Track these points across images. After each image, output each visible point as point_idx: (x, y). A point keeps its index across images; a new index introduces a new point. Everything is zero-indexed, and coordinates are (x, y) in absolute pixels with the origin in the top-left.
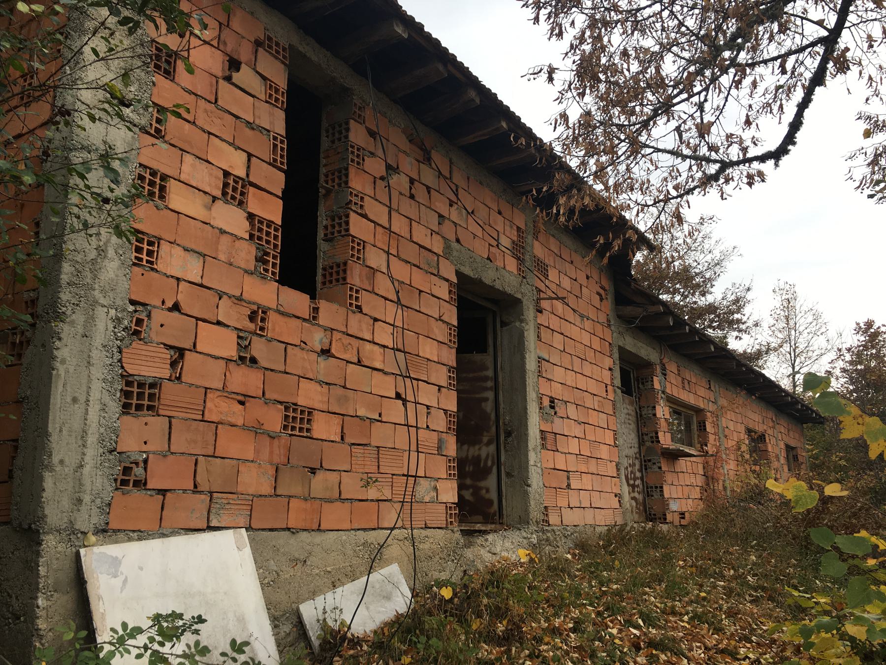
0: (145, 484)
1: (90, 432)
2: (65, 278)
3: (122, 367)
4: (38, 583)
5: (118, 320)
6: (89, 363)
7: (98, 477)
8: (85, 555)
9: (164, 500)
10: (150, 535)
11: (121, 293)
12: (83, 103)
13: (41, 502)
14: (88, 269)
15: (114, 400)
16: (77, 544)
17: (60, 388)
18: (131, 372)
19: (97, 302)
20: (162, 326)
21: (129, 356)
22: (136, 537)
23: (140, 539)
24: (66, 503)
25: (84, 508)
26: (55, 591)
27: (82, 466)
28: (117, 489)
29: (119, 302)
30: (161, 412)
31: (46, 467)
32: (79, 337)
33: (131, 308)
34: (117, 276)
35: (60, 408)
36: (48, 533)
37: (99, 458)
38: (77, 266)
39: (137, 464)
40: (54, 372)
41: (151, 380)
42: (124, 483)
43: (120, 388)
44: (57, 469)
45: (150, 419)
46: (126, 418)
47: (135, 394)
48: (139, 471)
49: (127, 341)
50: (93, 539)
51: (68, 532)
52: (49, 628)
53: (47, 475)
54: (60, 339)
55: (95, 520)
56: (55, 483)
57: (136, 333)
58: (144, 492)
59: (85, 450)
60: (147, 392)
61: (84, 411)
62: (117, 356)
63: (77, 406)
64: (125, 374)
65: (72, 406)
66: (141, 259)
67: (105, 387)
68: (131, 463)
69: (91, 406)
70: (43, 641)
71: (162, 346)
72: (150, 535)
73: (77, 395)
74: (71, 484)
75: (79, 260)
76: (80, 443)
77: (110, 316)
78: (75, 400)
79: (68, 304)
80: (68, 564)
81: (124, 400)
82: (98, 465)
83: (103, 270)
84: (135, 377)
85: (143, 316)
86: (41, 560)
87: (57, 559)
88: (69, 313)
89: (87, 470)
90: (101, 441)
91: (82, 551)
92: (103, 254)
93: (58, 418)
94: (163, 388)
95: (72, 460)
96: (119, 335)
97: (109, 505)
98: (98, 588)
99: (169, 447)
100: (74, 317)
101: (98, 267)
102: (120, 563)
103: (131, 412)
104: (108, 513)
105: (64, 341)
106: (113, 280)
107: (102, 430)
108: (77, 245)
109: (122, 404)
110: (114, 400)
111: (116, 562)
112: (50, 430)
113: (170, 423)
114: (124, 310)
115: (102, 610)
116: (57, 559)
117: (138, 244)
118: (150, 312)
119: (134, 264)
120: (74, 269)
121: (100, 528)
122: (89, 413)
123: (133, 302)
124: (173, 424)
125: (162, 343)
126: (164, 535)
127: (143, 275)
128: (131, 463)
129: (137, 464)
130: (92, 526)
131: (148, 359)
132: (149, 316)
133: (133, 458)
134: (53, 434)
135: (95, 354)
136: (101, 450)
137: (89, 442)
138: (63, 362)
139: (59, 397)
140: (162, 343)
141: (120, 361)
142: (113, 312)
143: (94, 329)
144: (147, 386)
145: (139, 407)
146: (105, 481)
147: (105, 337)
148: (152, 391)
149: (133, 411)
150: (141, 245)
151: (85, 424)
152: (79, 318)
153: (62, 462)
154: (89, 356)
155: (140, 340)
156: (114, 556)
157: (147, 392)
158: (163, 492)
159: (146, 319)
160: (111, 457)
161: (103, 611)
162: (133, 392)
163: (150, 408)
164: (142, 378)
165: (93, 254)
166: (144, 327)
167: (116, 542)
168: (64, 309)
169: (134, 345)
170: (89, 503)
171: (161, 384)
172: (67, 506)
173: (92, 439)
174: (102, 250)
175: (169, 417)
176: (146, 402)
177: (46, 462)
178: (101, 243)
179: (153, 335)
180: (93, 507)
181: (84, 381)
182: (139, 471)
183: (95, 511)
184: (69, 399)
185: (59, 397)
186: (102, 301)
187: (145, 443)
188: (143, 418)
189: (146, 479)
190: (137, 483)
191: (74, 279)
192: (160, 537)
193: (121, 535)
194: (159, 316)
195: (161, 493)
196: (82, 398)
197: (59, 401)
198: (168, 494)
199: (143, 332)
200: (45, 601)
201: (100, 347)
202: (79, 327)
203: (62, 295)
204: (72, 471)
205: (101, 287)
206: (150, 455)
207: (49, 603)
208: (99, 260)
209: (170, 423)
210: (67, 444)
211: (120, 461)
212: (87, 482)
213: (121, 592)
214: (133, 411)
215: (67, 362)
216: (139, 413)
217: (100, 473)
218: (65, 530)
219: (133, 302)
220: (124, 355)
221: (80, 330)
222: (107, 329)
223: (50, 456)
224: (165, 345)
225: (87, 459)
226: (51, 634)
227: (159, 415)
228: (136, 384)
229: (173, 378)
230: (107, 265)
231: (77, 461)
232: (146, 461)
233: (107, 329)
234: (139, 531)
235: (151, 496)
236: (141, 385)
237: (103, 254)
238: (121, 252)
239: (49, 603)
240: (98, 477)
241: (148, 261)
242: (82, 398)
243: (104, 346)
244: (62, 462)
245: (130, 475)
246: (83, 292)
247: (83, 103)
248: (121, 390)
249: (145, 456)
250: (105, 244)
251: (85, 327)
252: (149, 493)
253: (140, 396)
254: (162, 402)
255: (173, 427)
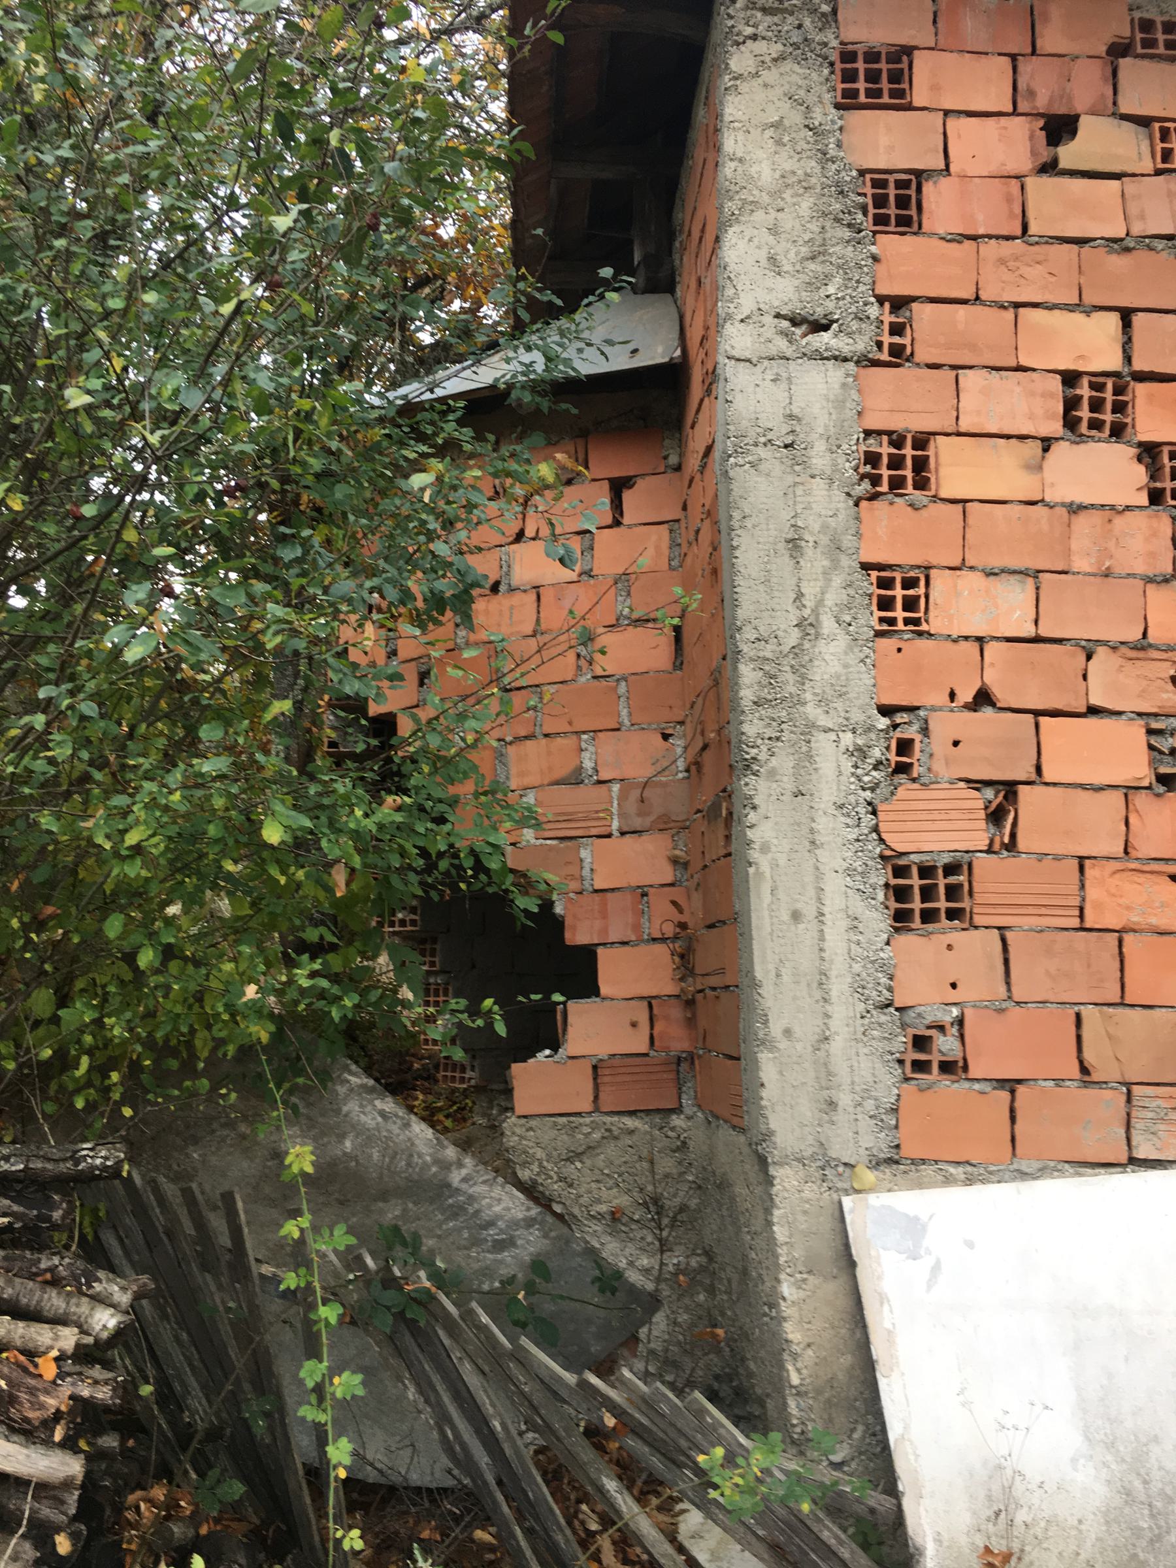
0: (965, 1068)
1: (833, 974)
2: (747, 695)
3: (881, 840)
4: (776, 1256)
5: (861, 752)
6: (813, 843)
7: (862, 1058)
8: (852, 1211)
9: (1013, 1100)
10: (991, 1173)
11: (857, 698)
12: (738, 360)
13: (762, 1108)
14: (788, 668)
15: (873, 906)
16: (840, 1185)
17: (767, 898)
18: (901, 848)
19: (814, 725)
20: (956, 744)
21: (892, 816)
22: (963, 1176)
23: (969, 1181)
24: (807, 1110)
25: (840, 1117)
26: (809, 1272)
27: (827, 1039)
28: (907, 1079)
29: (857, 716)
30: (978, 920)
31: (763, 1043)
32: (787, 797)
33: (883, 722)
34: (846, 666)
35: (771, 934)
36: (780, 1164)
37: (859, 1021)
38: (767, 668)
39: (941, 1028)
40: (751, 870)
41: (946, 859)
42: (921, 1066)
43: (882, 882)
44: (781, 1046)
45: (959, 938)
46: (903, 940)
47: (917, 891)
48: (946, 1045)
49: (884, 790)
50: (869, 1177)
51: (819, 1163)
52: (807, 1340)
53: (764, 1056)
54: (754, 808)
55: (867, 1141)
56: (781, 1073)
57: (902, 769)
58: (967, 1085)
59: (828, 1007)
60: (942, 882)
61: (816, 934)
62: (868, 820)
63: (801, 926)
64: (888, 853)
65: (793, 928)
66: (892, 622)
67: (851, 884)
68: (929, 1027)
69: (829, 923)
70: (799, 1365)
71: (962, 784)
72: (991, 1173)
73: (799, 906)
74: (812, 1074)
75: (769, 655)
76: (818, 994)
77: (842, 748)
78: (796, 916)
79: (759, 741)
80: (826, 1224)
81: (893, 904)
82: (859, 1036)
83: (816, 663)
84: (912, 857)
85: (911, 732)
86: (776, 1212)
87: (805, 1212)
88: (763, 757)
89: (837, 1046)
90: (859, 989)
91: (847, 1202)
92: (812, 631)
93: (769, 952)
94: (976, 871)
95: (806, 1030)
96: (866, 779)
97: (895, 1111)
98: (880, 1278)
99: (1009, 990)
100: (774, 762)
101: (807, 658)
102: (924, 1228)
103: (913, 926)
104: (896, 1127)
105: (761, 811)
106: (838, 677)
107: (857, 968)
108: (761, 629)
109: (892, 912)
110: (873, 906)
111: (914, 1228)
112: (759, 974)
113: (1004, 940)
114: (870, 729)
115: (887, 1325)
116: (805, 1212)
117: (883, 592)
118: (926, 721)
119: (879, 634)
120: (761, 673)
121: (882, 1156)
122: (827, 937)
123: (886, 711)
124: (1009, 941)
125: (961, 780)
126: (1023, 1175)
127: (899, 650)
128: (929, 1027)
129: (941, 1028)
130: (862, 1152)
131: (936, 816)
132: (925, 731)
133: (929, 1019)
134: (765, 982)
135: (823, 824)
136: (861, 1007)
137: (834, 993)
138: (765, 849)
139: (766, 913)
140: (961, 780)
141: (876, 829)
142: (847, 739)
143: (814, 777)
144: (940, 871)
145: (929, 916)
146: (878, 1065)
147: (839, 790)
148: (952, 880)
149: (917, 923)
150: (889, 593)
151: (822, 959)
152: (783, 762)
153: (788, 1032)
154: (812, 831)
155: (914, 780)
156: (912, 1214)
157: (942, 882)
158: (1010, 1085)
159: (918, 738)
160: (883, 1018)
161: (890, 1327)
162: (911, 886)
163: (952, 914)
164: (924, 857)
165: (792, 638)
166: (917, 754)
167: (920, 1185)
168: (754, 751)
169: (901, 793)
170: (851, 1110)
171: (970, 865)
172: (809, 1114)
173: (839, 987)
174: (811, 625)
175: (999, 928)
176: (942, 904)
177: (761, 1035)
178: (807, 612)
179: (938, 766)
180: (859, 1117)
181: (809, 879)
182: (946, 1045)
183: (866, 1124)
184: (785, 916)
185: (766, 913)
186: (824, 721)
187: (954, 986)
188: (942, 937)
189: (965, 1059)
190: (947, 1067)
191: (765, 693)
192: (1013, 1180)
193: (928, 1170)
194: (946, 726)
195: (1008, 1086)
196: (810, 911)
197: (767, 921)
198: (1021, 1090)
199: (916, 764)
200: (794, 1290)
201: (832, 810)
202: (785, 779)
203: (746, 728)
204: (810, 1049)
205: (815, 694)
206: (966, 1011)
207: (802, 1294)
208: (807, 645)
209: (1004, 940)
210: (795, 998)
211: (904, 1026)
212: (840, 1066)
213: (929, 1287)
214: (917, 923)
215: (773, 849)
216: (930, 927)
217: (866, 1050)
218: (813, 1158)
219: (886, 711)
220: (881, 815)
221: (789, 785)
222: (840, 774)
223: (765, 1023)
224: (968, 781)
225: (836, 1024)
226: (810, 1352)
227: (976, 927)
228: (915, 871)
229: (997, 847)
230: (824, 650)
231: (818, 1030)
232: (960, 1022)
233: (840, 774)
234: (968, 1163)
235: (982, 1093)
236: (926, 871)
237: (812, 631)
238: (848, 618)
239: (802, 1294)
240: (862, 1058)
241: (907, 622)
242: (810, 911)
243: (841, 806)
244: (788, 1032)
245: (930, 1052)
246: (784, 713)
247: (738, 360)
248: (887, 885)
249: (955, 1012)
250: (815, 611)
251: (796, 776)
252: (977, 1086)
253: (928, 893)
254: (978, 898)
255: (1011, 949)
